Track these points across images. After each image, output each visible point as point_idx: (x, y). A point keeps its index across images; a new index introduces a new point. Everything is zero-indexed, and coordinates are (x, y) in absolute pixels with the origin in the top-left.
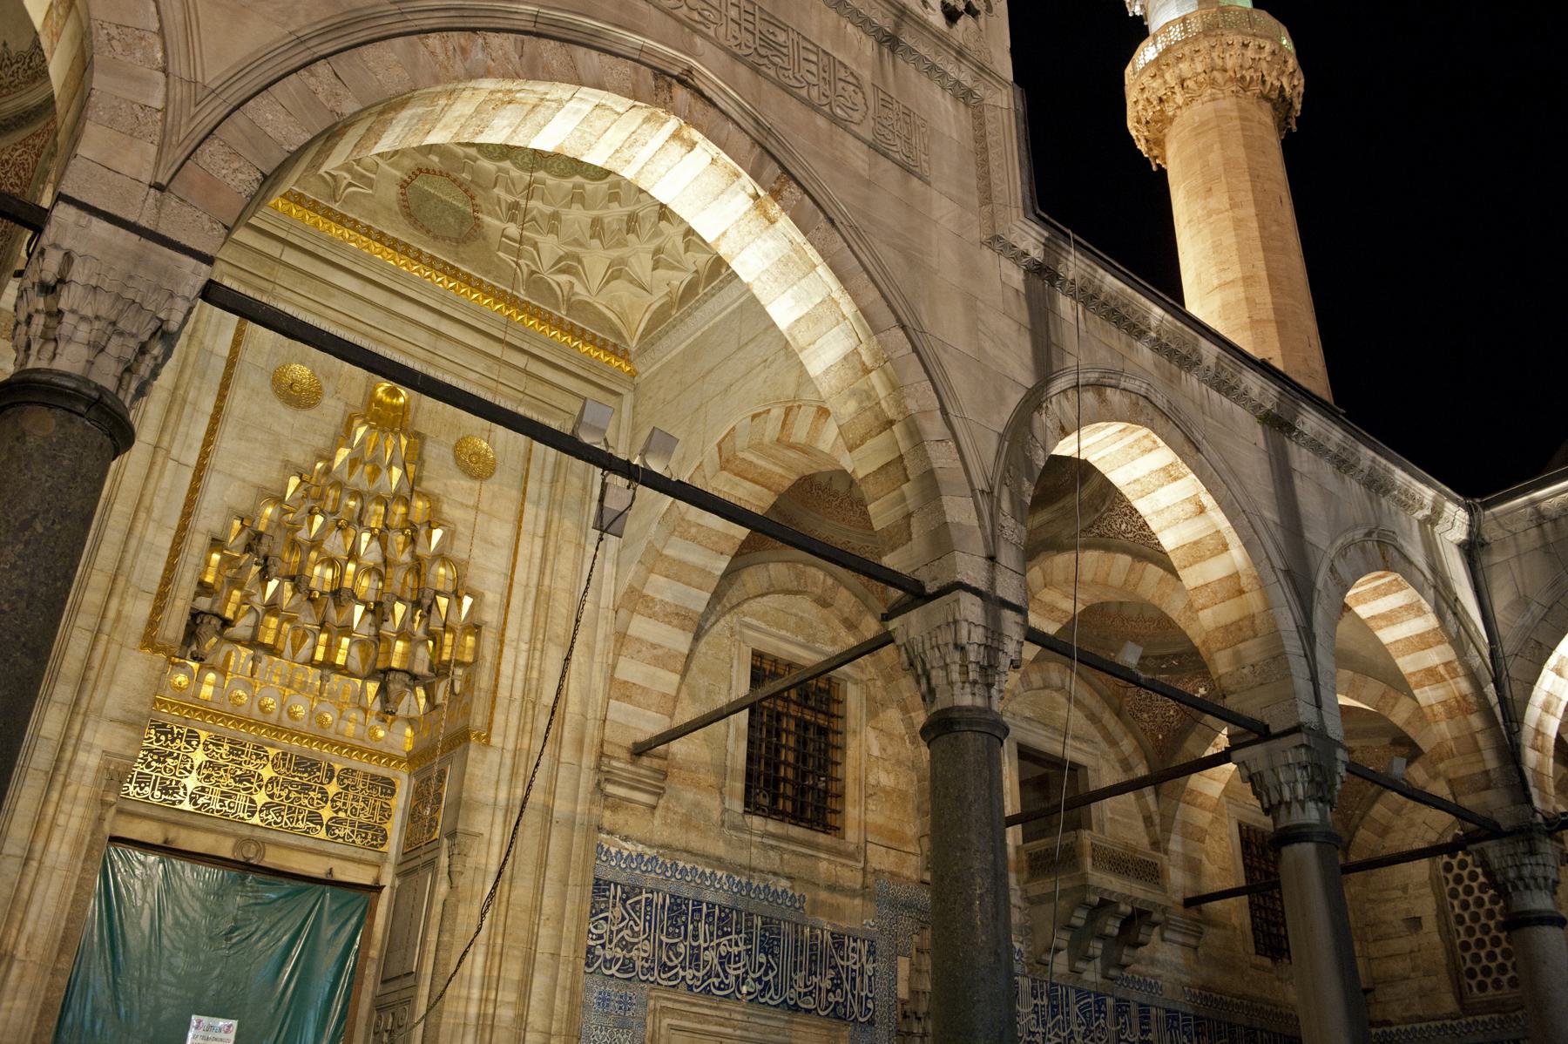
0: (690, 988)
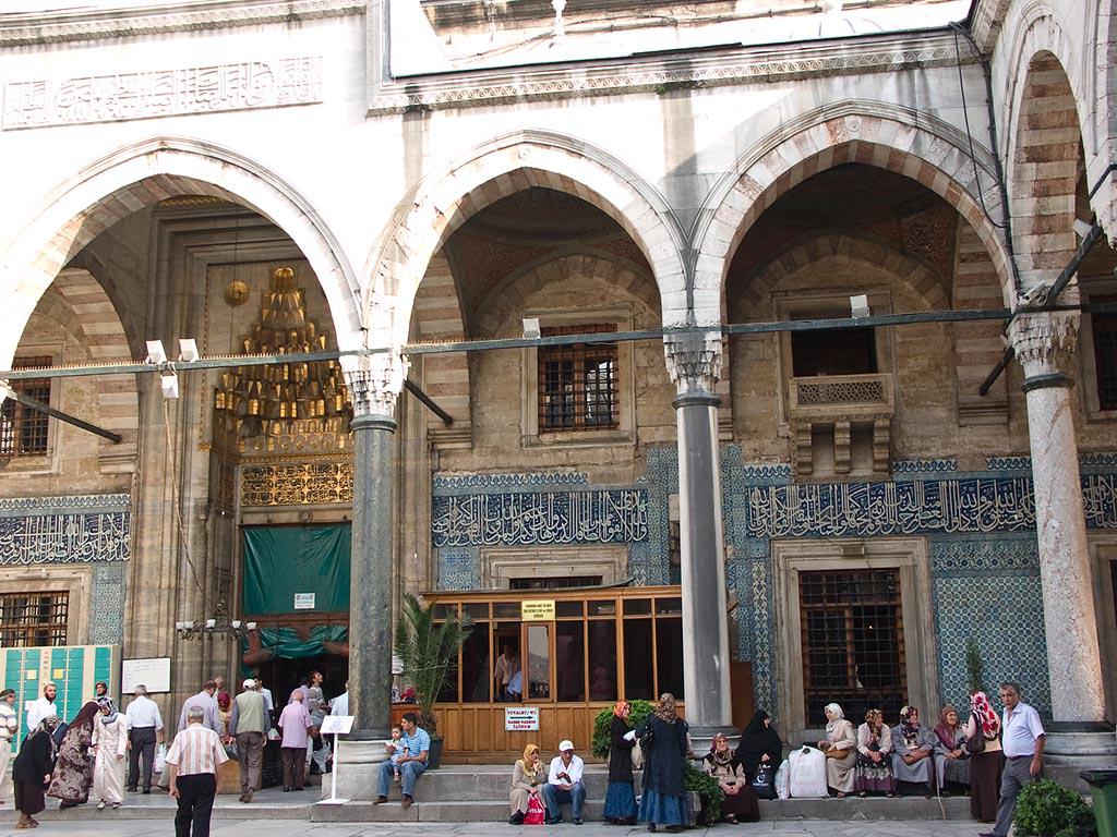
0: (506, 543)
